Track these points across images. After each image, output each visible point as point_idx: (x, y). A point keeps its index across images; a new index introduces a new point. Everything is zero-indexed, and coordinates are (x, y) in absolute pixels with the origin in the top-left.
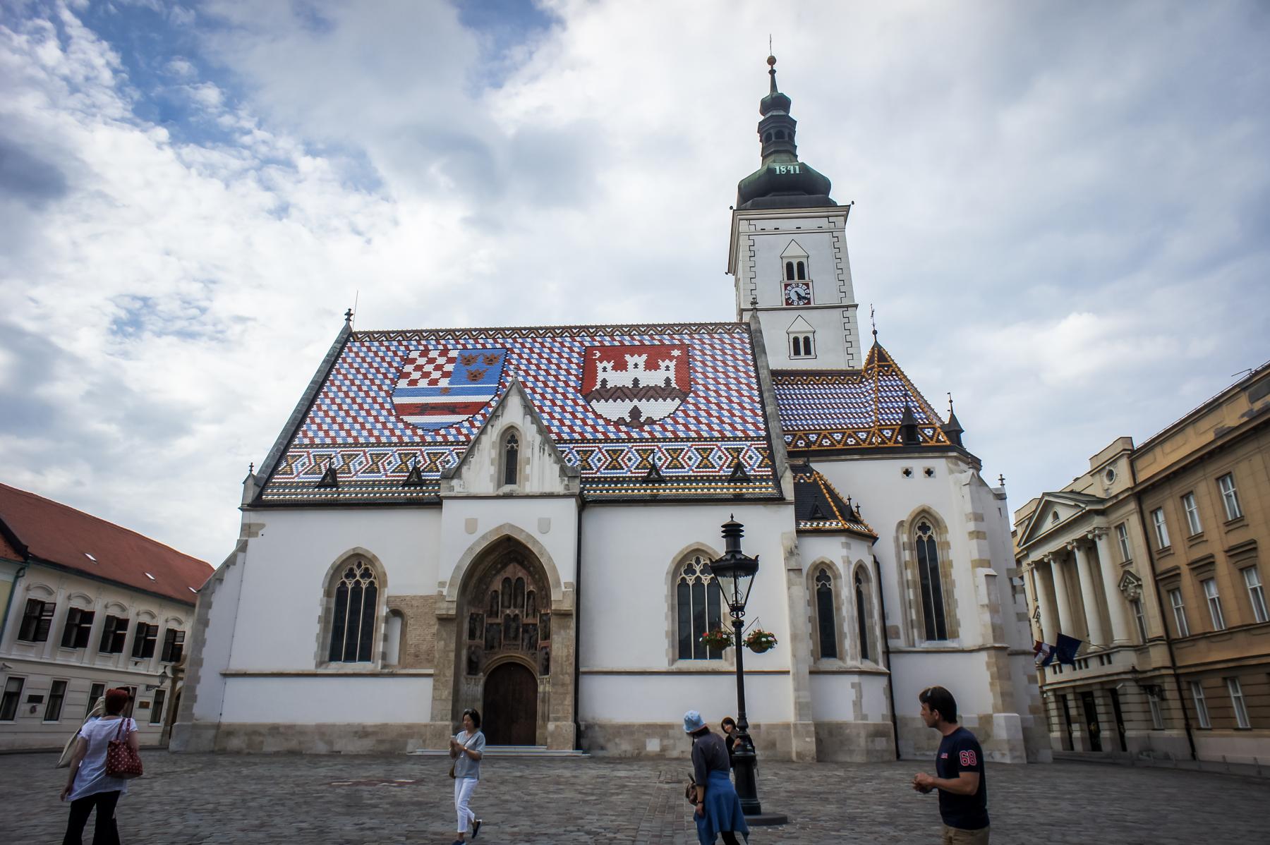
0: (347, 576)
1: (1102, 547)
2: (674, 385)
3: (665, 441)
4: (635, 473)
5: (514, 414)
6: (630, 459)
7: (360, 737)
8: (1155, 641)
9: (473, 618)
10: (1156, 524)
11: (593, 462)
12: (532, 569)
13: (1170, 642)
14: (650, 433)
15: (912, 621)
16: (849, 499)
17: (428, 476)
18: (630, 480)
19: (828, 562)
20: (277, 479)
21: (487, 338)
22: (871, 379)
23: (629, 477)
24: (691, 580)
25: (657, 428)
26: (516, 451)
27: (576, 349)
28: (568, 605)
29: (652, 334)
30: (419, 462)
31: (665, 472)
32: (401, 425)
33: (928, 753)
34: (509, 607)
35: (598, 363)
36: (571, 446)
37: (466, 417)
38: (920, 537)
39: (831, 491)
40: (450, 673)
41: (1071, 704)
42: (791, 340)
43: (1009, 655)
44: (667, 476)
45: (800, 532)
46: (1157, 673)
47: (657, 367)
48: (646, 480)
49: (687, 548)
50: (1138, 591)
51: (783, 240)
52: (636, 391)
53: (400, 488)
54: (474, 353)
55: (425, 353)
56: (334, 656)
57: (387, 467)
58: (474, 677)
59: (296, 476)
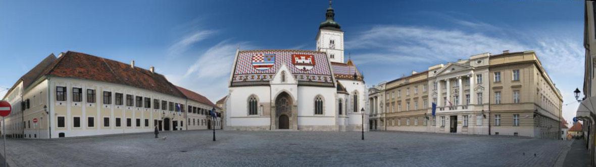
5: (284, 68)
13: (386, 114)
24: (317, 100)
45: (338, 93)
48: (308, 81)
52: (303, 64)
55: (257, 55)
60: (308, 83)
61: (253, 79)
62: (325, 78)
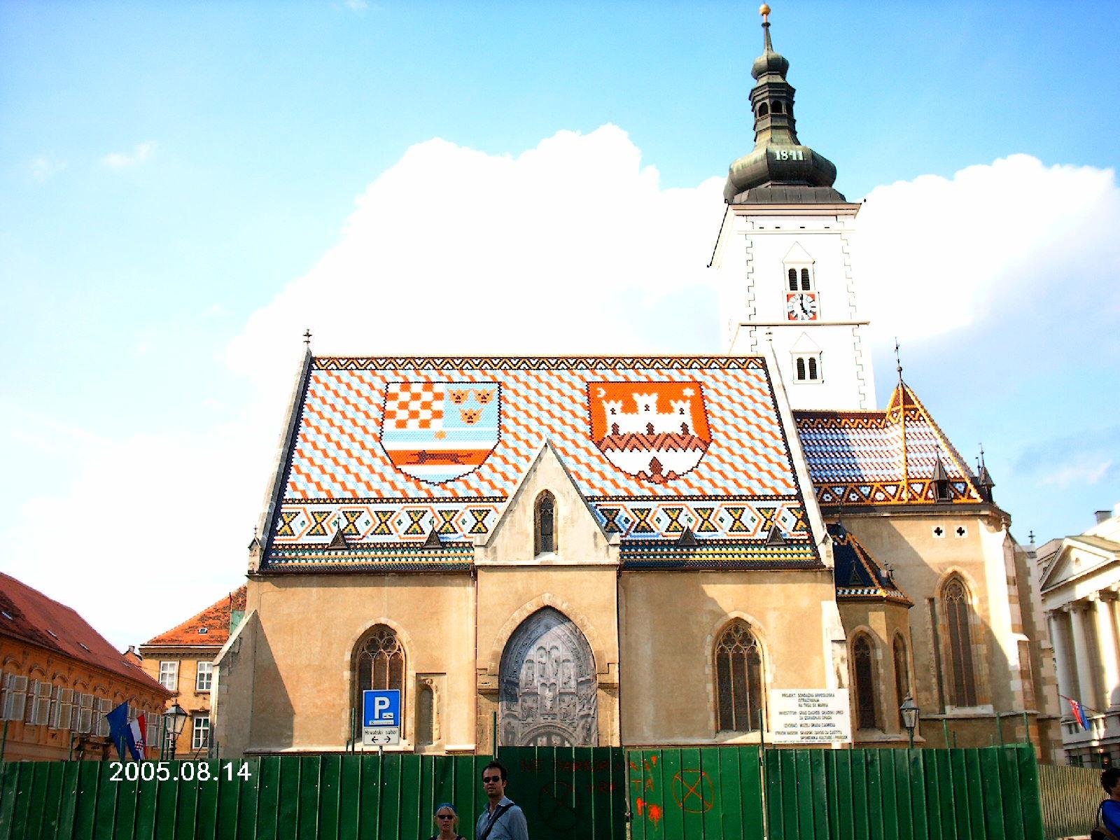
2: (692, 432)
14: (675, 489)
18: (662, 544)
20: (278, 540)
29: (658, 368)
32: (401, 477)
36: (594, 504)
37: (470, 468)
42: (796, 362)
45: (839, 600)
47: (669, 410)
48: (676, 544)
52: (650, 439)
53: (419, 553)
60: (673, 555)
61: (383, 529)
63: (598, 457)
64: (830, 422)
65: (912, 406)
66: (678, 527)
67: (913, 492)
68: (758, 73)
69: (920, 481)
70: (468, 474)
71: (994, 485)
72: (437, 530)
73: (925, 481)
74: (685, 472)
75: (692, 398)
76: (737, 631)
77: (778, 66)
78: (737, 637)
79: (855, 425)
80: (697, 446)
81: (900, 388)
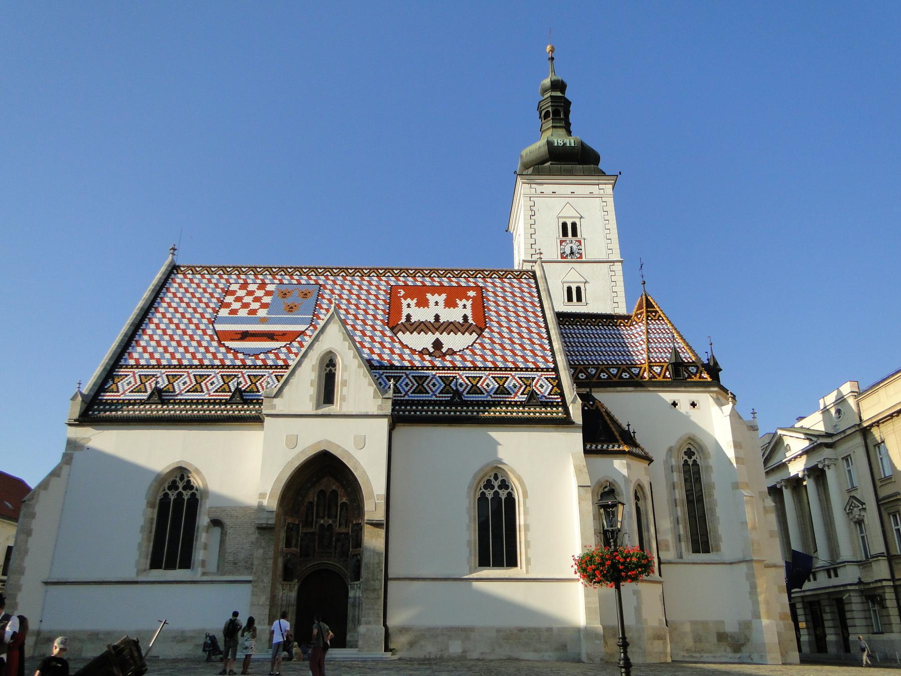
0: (170, 488)
1: (830, 474)
2: (471, 321)
3: (465, 370)
4: (440, 397)
6: (434, 385)
7: (179, 642)
8: (877, 557)
9: (291, 530)
10: (879, 457)
11: (401, 386)
12: (344, 482)
13: (891, 558)
14: (451, 362)
15: (679, 535)
16: (628, 425)
17: (250, 396)
18: (435, 403)
19: (611, 480)
21: (301, 275)
22: (641, 322)
23: (434, 400)
24: (489, 494)
25: (458, 358)
26: (334, 374)
27: (383, 288)
28: (380, 516)
29: (450, 277)
30: (241, 383)
31: (467, 397)
33: (695, 655)
34: (323, 518)
35: (403, 300)
36: (381, 372)
37: (283, 344)
38: (686, 461)
39: (612, 418)
40: (267, 580)
41: (800, 612)
43: (765, 567)
44: (468, 401)
45: (586, 452)
46: (879, 584)
47: (455, 305)
49: (488, 464)
50: (863, 513)
51: (558, 203)
52: (437, 325)
53: (223, 407)
54: (290, 288)
55: (244, 286)
56: (155, 564)
57: (210, 387)
58: (290, 583)
59: (122, 394)
62: (527, 382)
63: (391, 337)
64: (586, 321)
65: (653, 309)
66: (450, 390)
67: (653, 373)
68: (545, 91)
69: (659, 364)
70: (279, 348)
71: (721, 370)
72: (243, 389)
73: (663, 364)
74: (462, 349)
75: (473, 298)
76: (496, 477)
77: (559, 85)
78: (496, 484)
79: (608, 323)
80: (474, 331)
81: (644, 297)
